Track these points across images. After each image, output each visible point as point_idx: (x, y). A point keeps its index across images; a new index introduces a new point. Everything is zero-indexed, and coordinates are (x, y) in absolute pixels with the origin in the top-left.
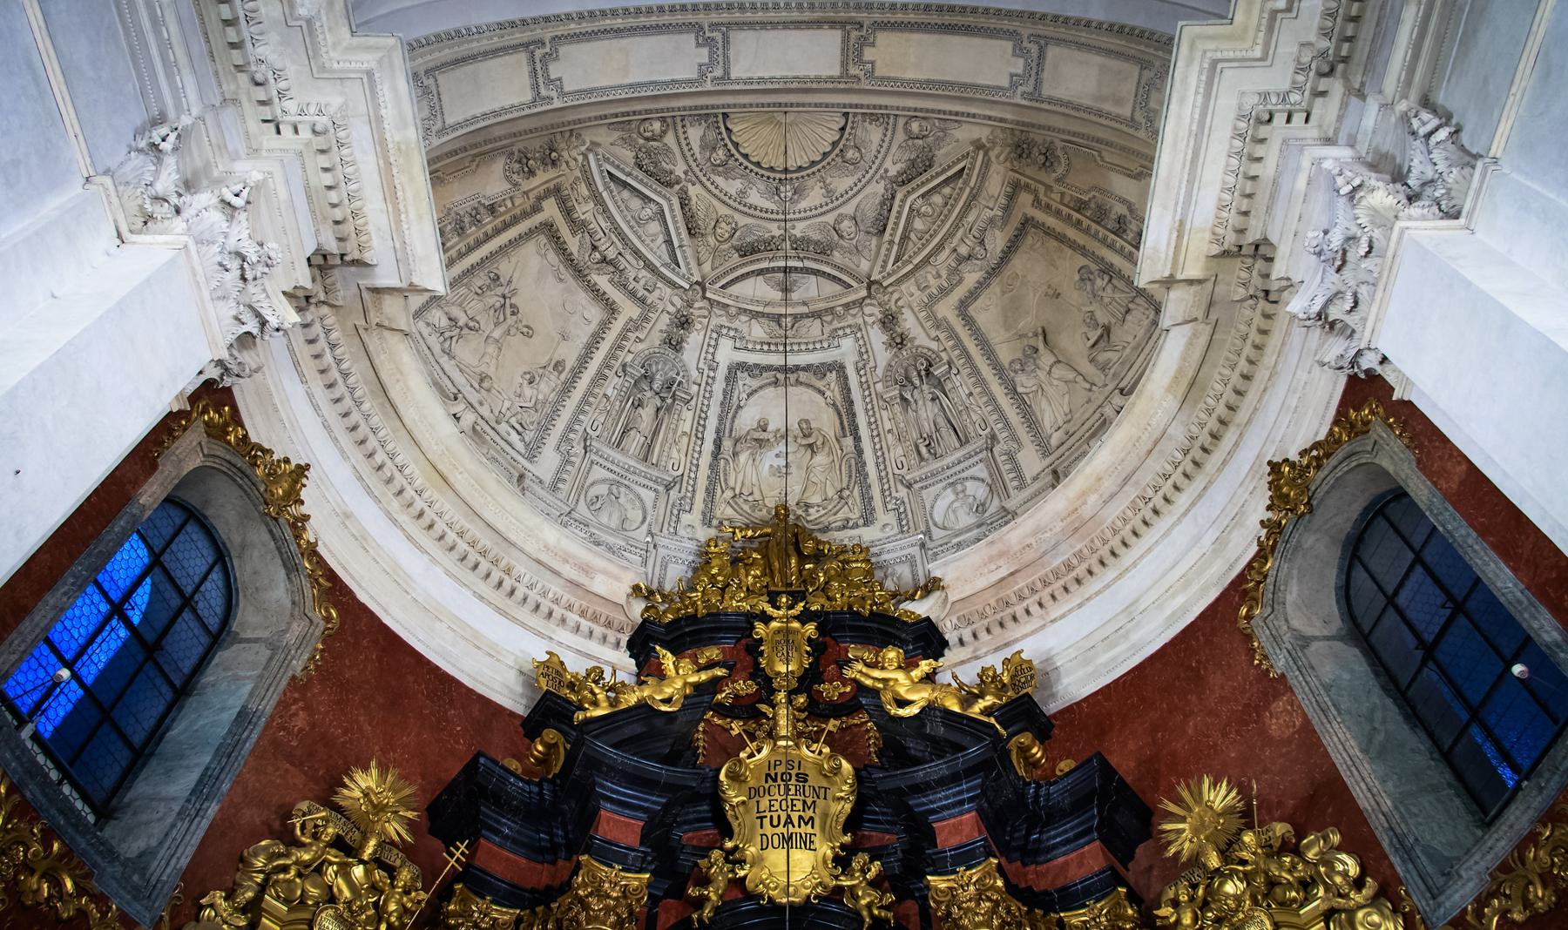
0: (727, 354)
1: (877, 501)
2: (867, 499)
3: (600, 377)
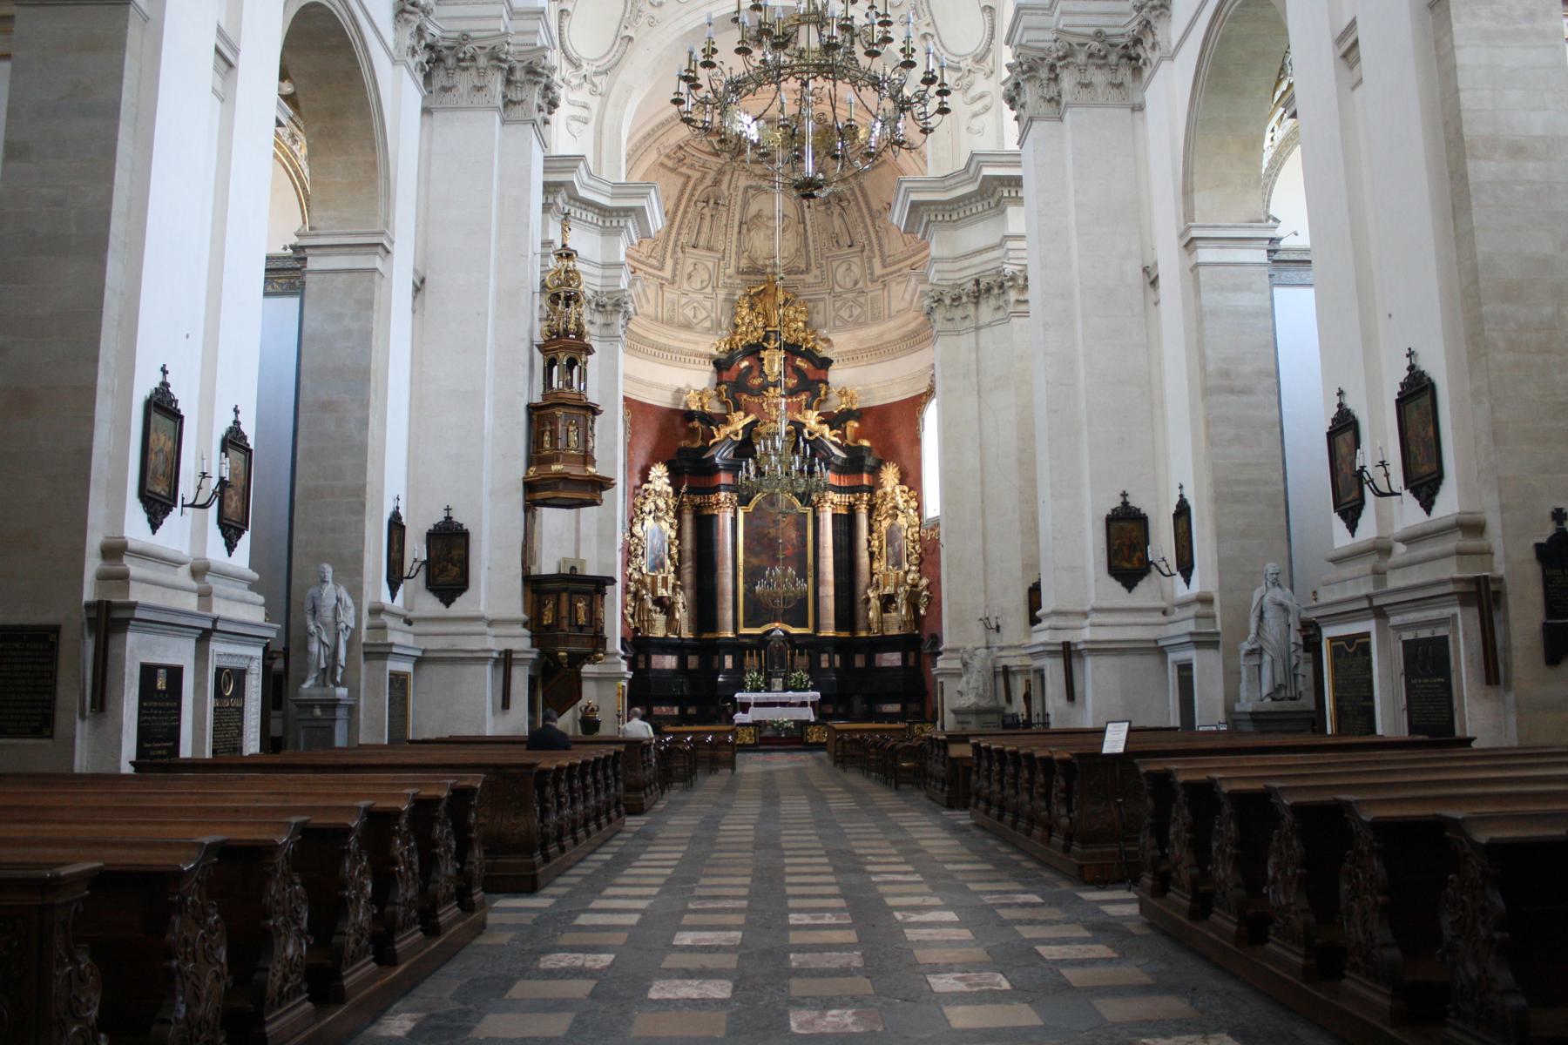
0: (743, 182)
1: (813, 261)
3: (685, 212)
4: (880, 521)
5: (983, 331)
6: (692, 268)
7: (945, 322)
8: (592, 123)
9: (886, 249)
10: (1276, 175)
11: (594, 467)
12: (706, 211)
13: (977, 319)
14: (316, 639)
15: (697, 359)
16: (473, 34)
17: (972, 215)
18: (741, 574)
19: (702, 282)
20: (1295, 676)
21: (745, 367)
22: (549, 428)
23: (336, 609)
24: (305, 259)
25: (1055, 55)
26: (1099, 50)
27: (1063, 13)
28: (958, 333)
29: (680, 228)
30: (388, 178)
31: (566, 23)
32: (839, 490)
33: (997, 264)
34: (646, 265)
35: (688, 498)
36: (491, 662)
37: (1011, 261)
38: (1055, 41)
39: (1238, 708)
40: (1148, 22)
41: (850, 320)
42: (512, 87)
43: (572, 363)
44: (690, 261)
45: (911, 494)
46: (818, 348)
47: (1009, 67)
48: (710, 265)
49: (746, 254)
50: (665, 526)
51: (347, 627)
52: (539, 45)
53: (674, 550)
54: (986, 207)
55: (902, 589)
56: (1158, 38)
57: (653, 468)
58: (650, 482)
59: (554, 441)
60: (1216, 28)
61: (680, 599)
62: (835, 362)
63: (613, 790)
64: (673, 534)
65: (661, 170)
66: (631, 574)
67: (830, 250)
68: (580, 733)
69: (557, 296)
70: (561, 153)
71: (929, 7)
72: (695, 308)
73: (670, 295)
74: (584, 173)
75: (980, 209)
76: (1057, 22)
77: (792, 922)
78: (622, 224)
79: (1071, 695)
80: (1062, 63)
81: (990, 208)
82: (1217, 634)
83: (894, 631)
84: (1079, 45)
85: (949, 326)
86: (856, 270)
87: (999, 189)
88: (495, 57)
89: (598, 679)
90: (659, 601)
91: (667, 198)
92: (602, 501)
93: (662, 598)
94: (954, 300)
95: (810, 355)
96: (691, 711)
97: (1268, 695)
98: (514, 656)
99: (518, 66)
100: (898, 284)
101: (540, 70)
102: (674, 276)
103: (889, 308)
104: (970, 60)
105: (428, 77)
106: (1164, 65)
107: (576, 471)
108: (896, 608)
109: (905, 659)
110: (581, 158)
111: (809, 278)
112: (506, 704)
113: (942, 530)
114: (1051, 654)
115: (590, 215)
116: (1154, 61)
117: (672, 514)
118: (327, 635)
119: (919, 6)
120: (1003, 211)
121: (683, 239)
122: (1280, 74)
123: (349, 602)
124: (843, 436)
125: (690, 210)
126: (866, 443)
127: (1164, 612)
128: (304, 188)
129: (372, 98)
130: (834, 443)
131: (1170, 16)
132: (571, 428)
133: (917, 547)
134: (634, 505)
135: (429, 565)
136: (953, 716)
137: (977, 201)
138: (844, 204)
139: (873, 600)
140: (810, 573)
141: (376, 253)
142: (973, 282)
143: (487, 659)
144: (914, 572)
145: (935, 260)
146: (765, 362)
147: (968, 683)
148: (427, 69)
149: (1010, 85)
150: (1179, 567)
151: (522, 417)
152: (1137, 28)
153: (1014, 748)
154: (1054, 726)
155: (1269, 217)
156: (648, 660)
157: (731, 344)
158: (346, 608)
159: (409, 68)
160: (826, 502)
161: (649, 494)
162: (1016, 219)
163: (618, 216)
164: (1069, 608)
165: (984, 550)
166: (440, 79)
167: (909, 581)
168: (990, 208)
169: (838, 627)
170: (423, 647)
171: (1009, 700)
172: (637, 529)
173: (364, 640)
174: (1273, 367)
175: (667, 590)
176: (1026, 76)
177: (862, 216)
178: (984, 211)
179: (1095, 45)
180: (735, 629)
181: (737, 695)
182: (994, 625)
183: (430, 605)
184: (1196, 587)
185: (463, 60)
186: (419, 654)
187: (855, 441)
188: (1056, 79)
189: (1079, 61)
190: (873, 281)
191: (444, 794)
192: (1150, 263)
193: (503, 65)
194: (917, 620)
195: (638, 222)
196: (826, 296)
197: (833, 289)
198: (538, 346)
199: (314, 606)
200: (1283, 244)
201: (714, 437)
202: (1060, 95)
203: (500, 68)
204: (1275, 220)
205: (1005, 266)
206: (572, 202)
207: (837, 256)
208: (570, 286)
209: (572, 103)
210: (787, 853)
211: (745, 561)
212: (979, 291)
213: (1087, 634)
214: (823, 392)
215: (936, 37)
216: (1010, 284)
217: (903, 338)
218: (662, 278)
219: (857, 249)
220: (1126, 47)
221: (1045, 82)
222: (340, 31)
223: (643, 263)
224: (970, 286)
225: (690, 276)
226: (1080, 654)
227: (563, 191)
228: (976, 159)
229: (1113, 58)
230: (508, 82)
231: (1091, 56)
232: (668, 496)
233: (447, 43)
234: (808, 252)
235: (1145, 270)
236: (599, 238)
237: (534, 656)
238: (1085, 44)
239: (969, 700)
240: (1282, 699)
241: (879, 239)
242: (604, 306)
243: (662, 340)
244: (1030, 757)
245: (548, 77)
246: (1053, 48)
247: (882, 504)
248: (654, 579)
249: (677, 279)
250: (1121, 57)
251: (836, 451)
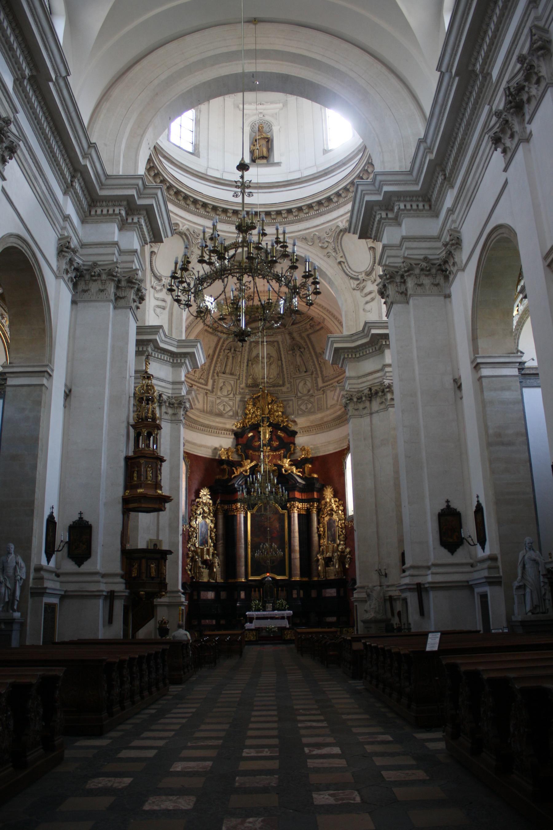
1: (286, 380)
2: (284, 379)
3: (219, 355)
4: (324, 518)
5: (374, 415)
6: (222, 384)
7: (354, 411)
8: (167, 309)
9: (324, 373)
10: (521, 329)
11: (161, 490)
12: (230, 354)
13: (371, 409)
14: (3, 585)
15: (225, 432)
16: (99, 263)
17: (367, 354)
18: (249, 547)
19: (228, 391)
20: (544, 600)
21: (251, 436)
22: (136, 469)
23: (15, 569)
24: (6, 379)
25: (403, 270)
26: (426, 267)
27: (407, 248)
28: (361, 416)
29: (216, 363)
30: (51, 337)
31: (154, 258)
32: (301, 501)
33: (380, 379)
34: (199, 383)
35: (221, 506)
36: (102, 598)
37: (388, 378)
38: (403, 263)
39: (514, 619)
40: (451, 252)
41: (306, 410)
42: (120, 290)
43: (149, 434)
44: (221, 381)
45: (340, 502)
46: (290, 425)
47: (380, 276)
48: (232, 382)
49: (251, 377)
50: (208, 521)
51: (21, 578)
52: (134, 268)
53: (213, 534)
54: (374, 350)
55: (336, 554)
56: (456, 260)
57: (202, 491)
58: (200, 498)
59: (139, 477)
60: (485, 254)
61: (216, 561)
62: (299, 433)
63: (161, 671)
64: (212, 526)
65: (206, 333)
66: (190, 547)
67: (295, 374)
68: (159, 637)
69: (142, 399)
70: (150, 324)
71: (342, 248)
72: (224, 405)
73: (211, 399)
74: (162, 335)
75: (371, 351)
76: (404, 253)
77: (244, 754)
78: (183, 361)
79: (422, 612)
80: (407, 274)
81: (376, 350)
82: (501, 577)
83: (332, 577)
84: (416, 264)
85: (356, 413)
86: (309, 384)
87: (380, 340)
88: (111, 274)
89: (169, 606)
90: (205, 562)
91: (209, 348)
92: (165, 508)
93: (207, 560)
94: (358, 399)
95: (285, 429)
96: (223, 622)
97: (530, 611)
98: (116, 594)
99: (123, 279)
100: (331, 391)
101: (134, 281)
102: (213, 388)
103: (327, 404)
104: (363, 274)
105: (75, 285)
106: (459, 274)
107: (151, 492)
108: (333, 564)
109: (338, 592)
110: (161, 327)
111: (284, 389)
112: (110, 621)
113: (355, 522)
114: (410, 590)
115: (166, 357)
116: (454, 272)
117: (212, 515)
118: (10, 583)
119: (337, 247)
120: (383, 352)
121: (218, 369)
122: (519, 277)
123: (23, 564)
124: (303, 472)
125: (221, 354)
126: (316, 476)
127: (472, 566)
128: (7, 342)
129: (43, 296)
130: (299, 476)
131: (461, 249)
132: (149, 469)
133: (344, 531)
134: (192, 510)
135: (70, 544)
136: (362, 624)
137: (369, 347)
138: (302, 350)
139: (320, 560)
140: (287, 546)
141: (44, 376)
142: (368, 389)
143: (100, 596)
144: (343, 545)
145: (349, 378)
146: (262, 433)
147: (370, 605)
148: (75, 280)
149: (381, 286)
150: (478, 541)
151: (122, 463)
152: (445, 256)
153: (382, 646)
154: (413, 630)
155: (518, 351)
156: (199, 595)
157: (243, 424)
158: (21, 568)
159: (64, 280)
160: (294, 507)
161: (200, 504)
162: (388, 357)
163: (181, 357)
164: (420, 564)
165: (378, 532)
166: (82, 286)
167: (340, 550)
168: (376, 350)
169: (302, 575)
170: (65, 589)
171: (393, 614)
172: (193, 523)
173: (31, 585)
174: (524, 431)
175: (209, 556)
176: (388, 281)
177: (311, 356)
178: (373, 352)
179: (424, 264)
180: (246, 577)
181: (247, 613)
182: (384, 574)
183: (69, 566)
184: (488, 551)
185: (94, 276)
186: (63, 593)
187: (310, 475)
188: (404, 282)
189: (416, 272)
190: (318, 390)
191: (34, 681)
192: (457, 377)
193: (115, 278)
194: (344, 571)
195: (192, 361)
196: (293, 398)
197: (297, 394)
198: (132, 425)
199: (3, 567)
200: (527, 365)
201: (234, 473)
202: (406, 290)
203: (113, 280)
204: (522, 352)
205: (384, 381)
206: (156, 350)
207: (299, 377)
208: (149, 393)
209: (157, 299)
210: (255, 708)
211: (251, 539)
212: (371, 394)
213: (430, 579)
214: (292, 449)
215: (346, 263)
216: (388, 390)
217: (334, 420)
218: (207, 390)
219: (309, 373)
220: (440, 265)
221: (399, 284)
222: (26, 261)
223: (196, 382)
224: (367, 392)
225: (221, 388)
226: (426, 589)
227: (151, 344)
228: (368, 325)
229: (434, 271)
230: (118, 287)
231: (422, 270)
232: (210, 505)
233: (85, 268)
234: (283, 375)
235: (455, 381)
236: (170, 369)
237: (127, 594)
238: (418, 264)
239: (371, 615)
240: (538, 613)
241: (320, 368)
242: (173, 404)
243: (207, 422)
244: (389, 651)
245: (139, 285)
246: (402, 267)
247: (324, 508)
248: (202, 550)
249: (215, 390)
250: (438, 270)
251: (300, 480)
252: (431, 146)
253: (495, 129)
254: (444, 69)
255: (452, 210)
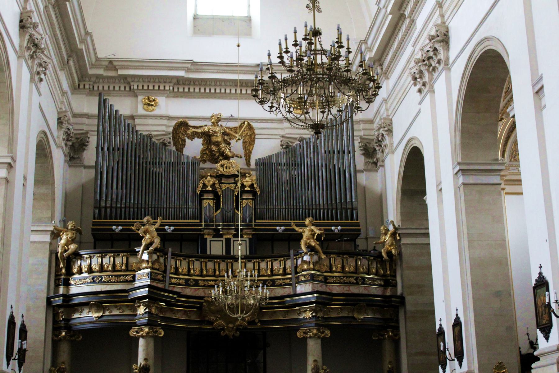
252: (371, 47)
253: (414, 70)
254: (381, 6)
255: (386, 100)
